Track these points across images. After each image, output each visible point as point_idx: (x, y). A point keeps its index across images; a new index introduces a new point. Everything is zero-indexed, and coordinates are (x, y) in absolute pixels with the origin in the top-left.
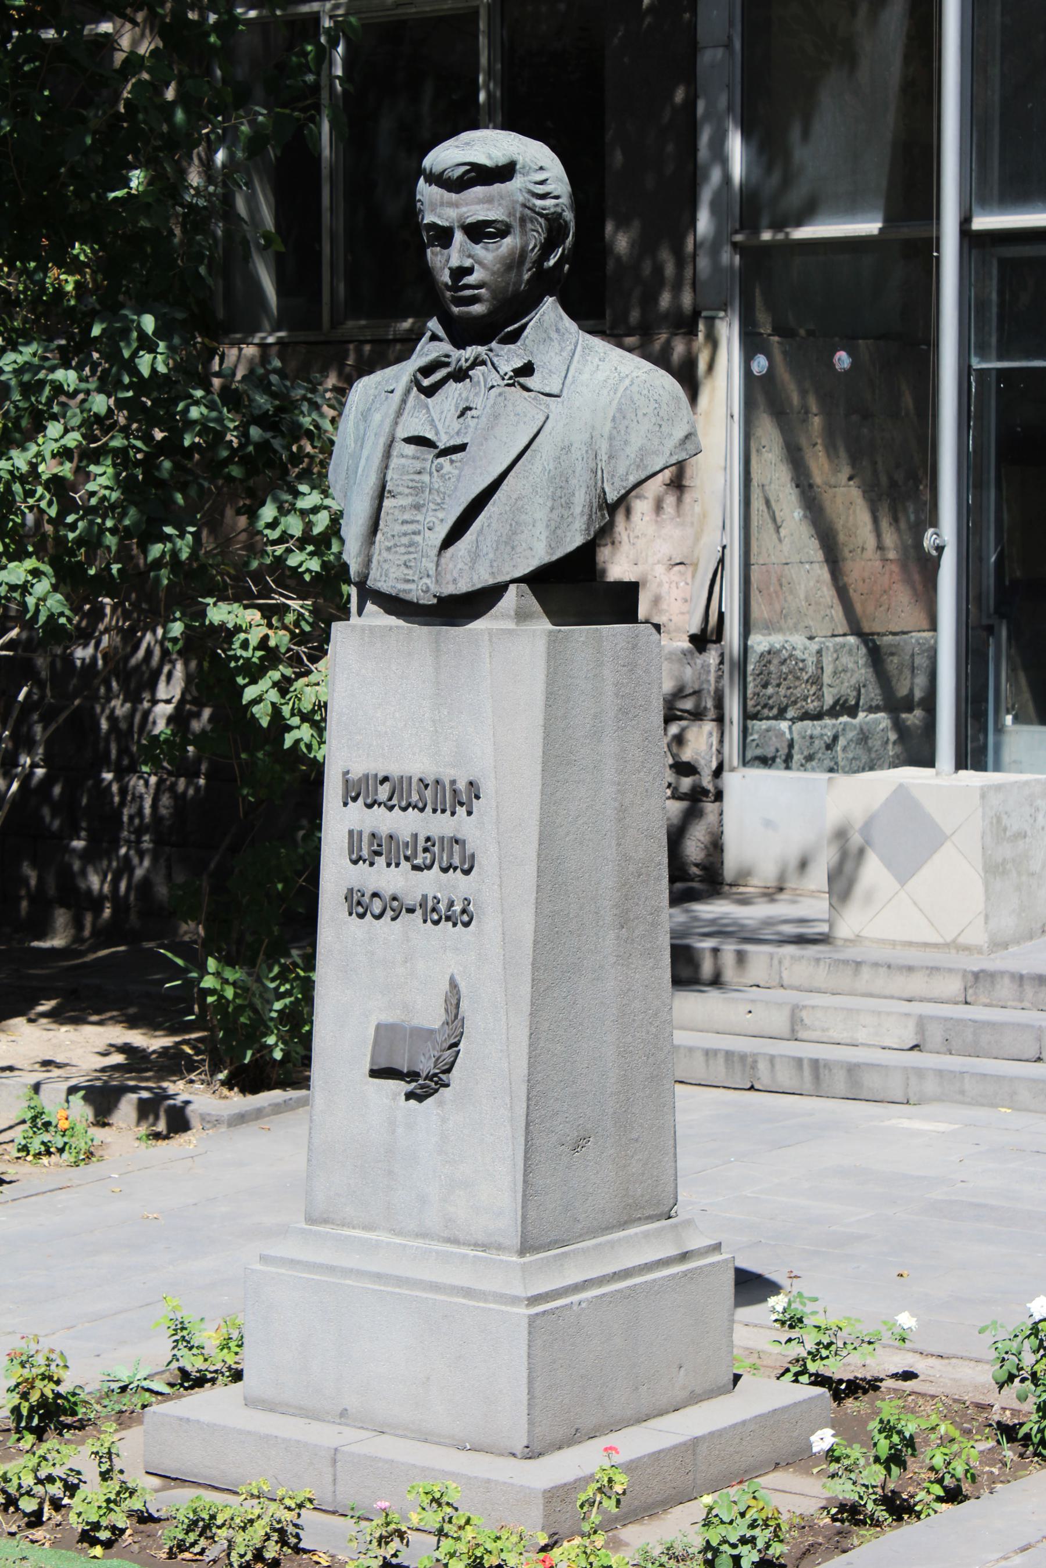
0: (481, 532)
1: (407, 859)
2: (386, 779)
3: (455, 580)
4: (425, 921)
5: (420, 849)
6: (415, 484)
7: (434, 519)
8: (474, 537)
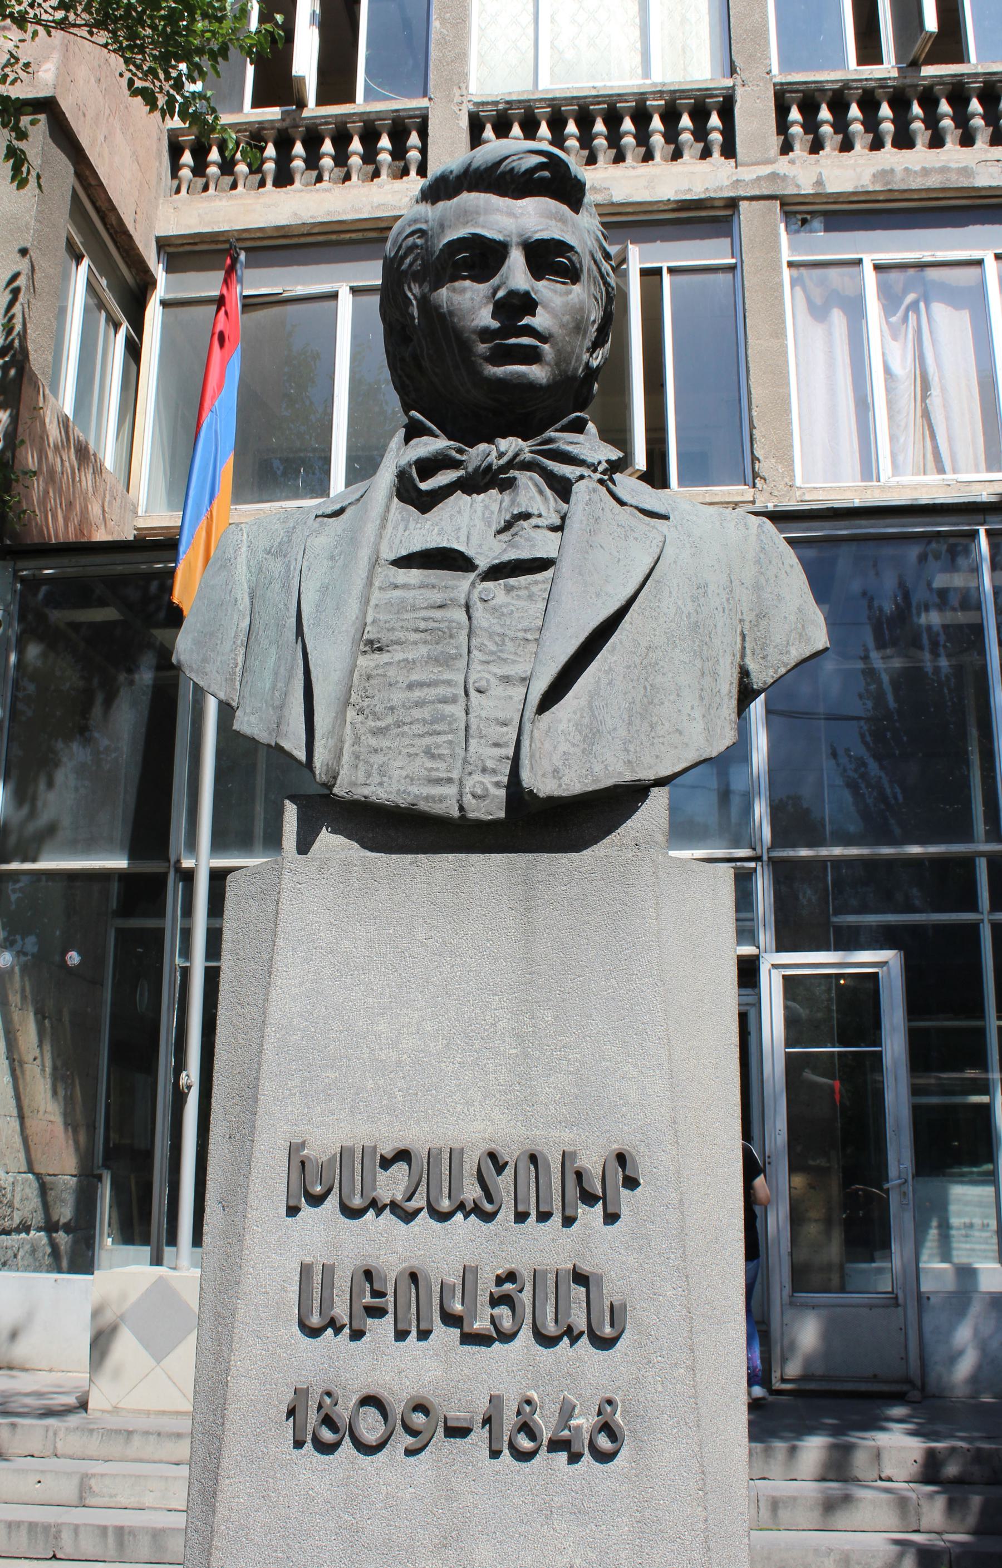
0: (594, 694)
1: (451, 1319)
2: (403, 1155)
3: (556, 771)
4: (495, 1454)
5: (484, 1299)
6: (431, 625)
7: (486, 675)
8: (583, 702)
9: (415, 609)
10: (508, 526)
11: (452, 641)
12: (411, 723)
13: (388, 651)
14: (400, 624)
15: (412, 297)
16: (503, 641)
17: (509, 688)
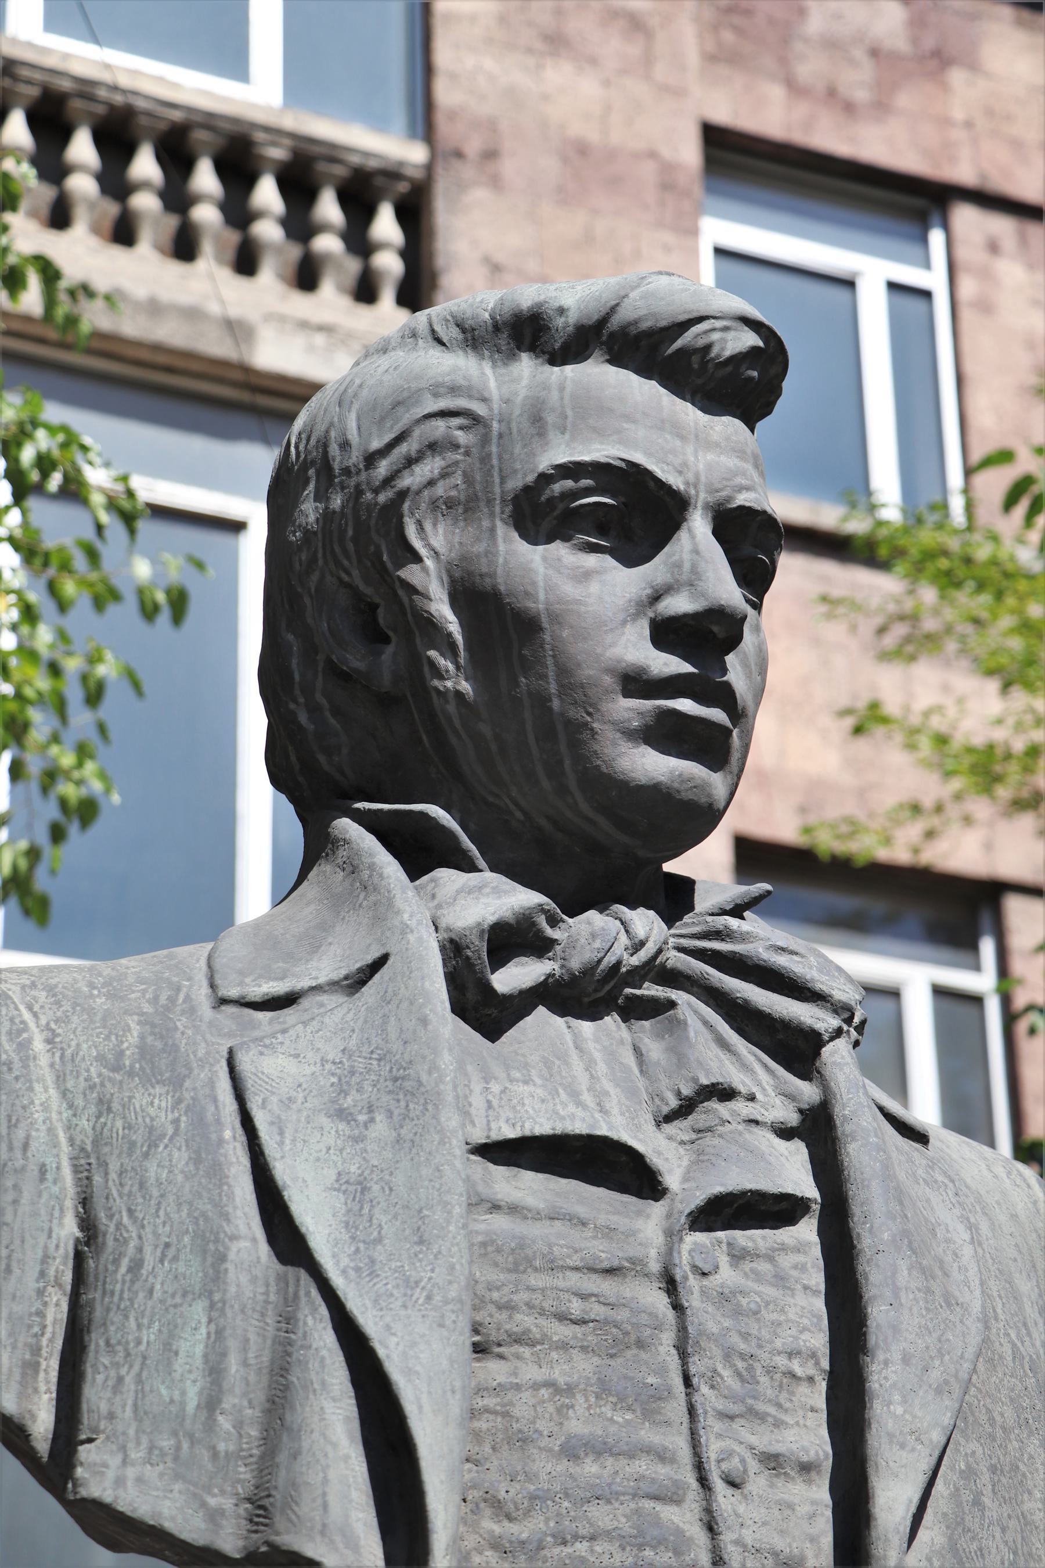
6: (597, 1311)
9: (553, 1266)
10: (686, 1108)
11: (643, 1355)
12: (592, 1538)
13: (501, 1357)
14: (524, 1296)
15: (423, 552)
16: (750, 1369)
17: (780, 1482)
